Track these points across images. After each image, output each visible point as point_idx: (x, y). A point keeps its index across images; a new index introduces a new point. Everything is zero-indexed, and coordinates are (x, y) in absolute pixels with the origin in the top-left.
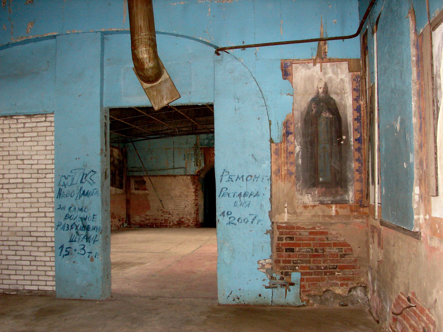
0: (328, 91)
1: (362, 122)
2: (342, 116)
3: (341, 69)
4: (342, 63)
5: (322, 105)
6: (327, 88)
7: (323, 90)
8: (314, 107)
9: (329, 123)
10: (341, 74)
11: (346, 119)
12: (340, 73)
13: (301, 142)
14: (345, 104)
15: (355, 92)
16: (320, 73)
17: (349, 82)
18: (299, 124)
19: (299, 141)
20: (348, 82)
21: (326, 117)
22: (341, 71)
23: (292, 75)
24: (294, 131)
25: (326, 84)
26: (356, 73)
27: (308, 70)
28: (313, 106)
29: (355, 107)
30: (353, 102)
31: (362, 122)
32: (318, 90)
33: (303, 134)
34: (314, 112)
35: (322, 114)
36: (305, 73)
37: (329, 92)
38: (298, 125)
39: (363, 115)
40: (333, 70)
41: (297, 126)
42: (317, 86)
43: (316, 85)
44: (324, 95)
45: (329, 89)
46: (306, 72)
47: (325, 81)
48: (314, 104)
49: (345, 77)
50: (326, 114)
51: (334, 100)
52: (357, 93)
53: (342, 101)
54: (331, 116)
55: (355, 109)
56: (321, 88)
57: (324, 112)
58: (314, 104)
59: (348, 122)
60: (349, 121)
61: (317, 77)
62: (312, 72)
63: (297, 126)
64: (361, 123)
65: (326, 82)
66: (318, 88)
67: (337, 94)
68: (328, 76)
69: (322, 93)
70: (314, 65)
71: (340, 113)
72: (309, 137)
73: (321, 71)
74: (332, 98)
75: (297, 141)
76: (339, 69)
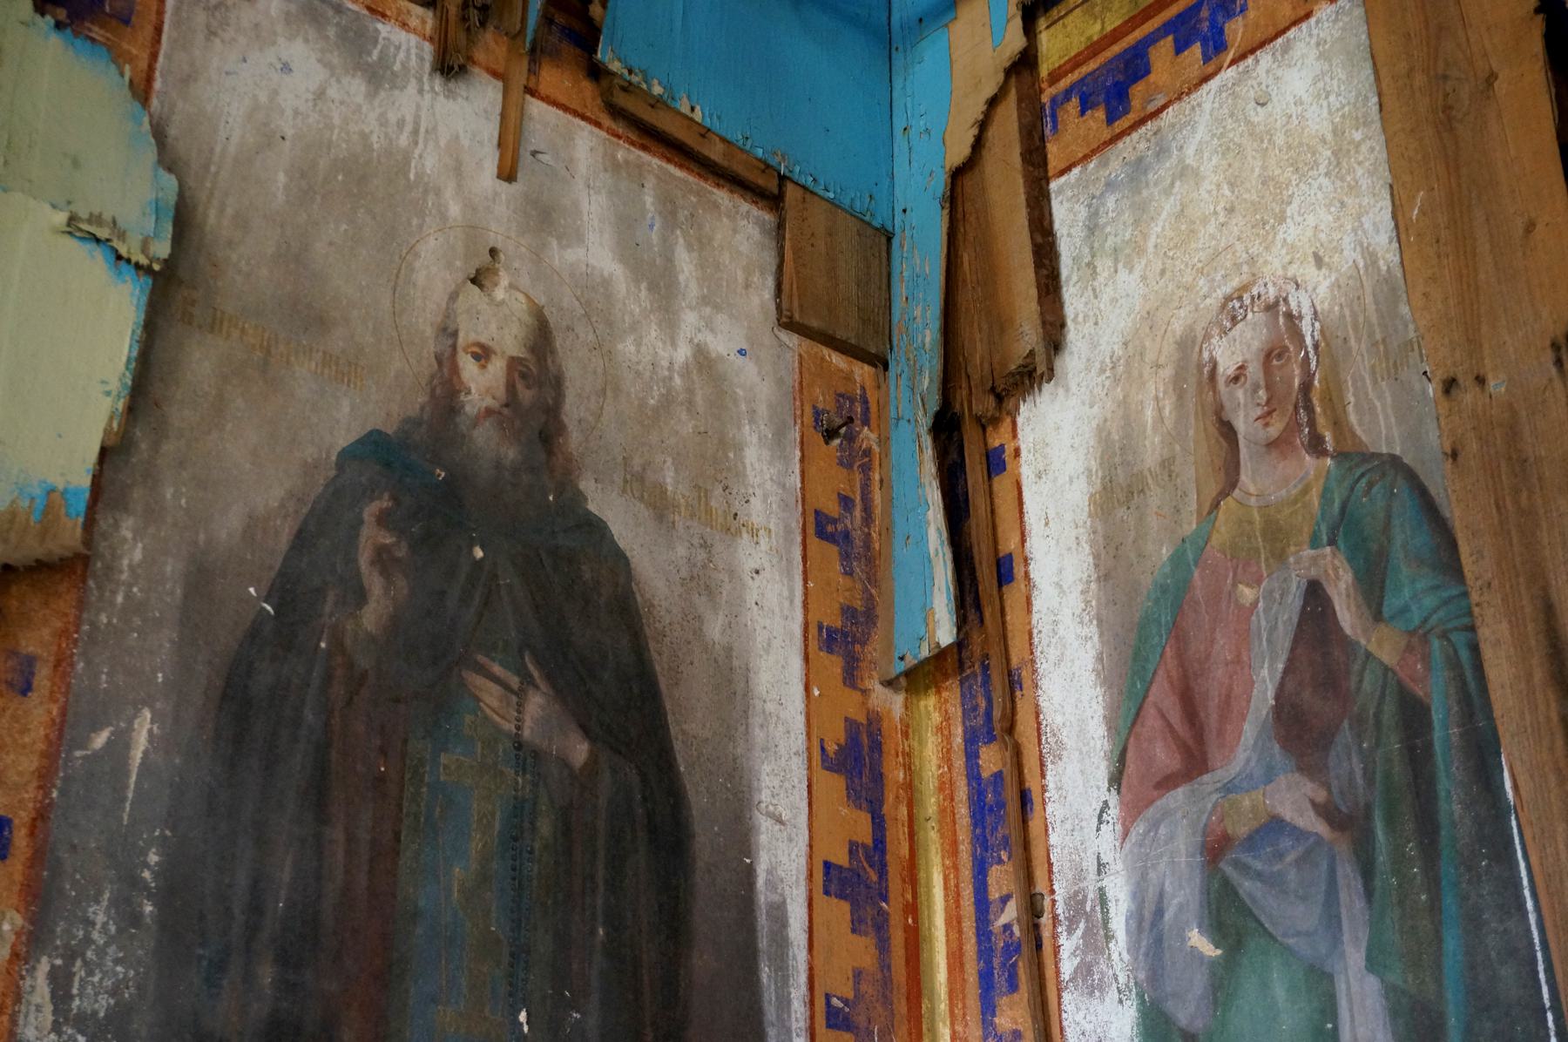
0: (561, 429)
1: (897, 938)
2: (698, 798)
3: (701, 244)
4: (722, 196)
5: (479, 564)
6: (558, 383)
7: (511, 387)
8: (382, 558)
9: (545, 827)
10: (705, 300)
11: (742, 840)
12: (693, 291)
13: (120, 1016)
14: (729, 650)
15: (833, 551)
16: (485, 177)
17: (780, 434)
18: (143, 730)
19: (103, 1004)
20: (763, 410)
21: (519, 745)
22: (701, 266)
23: (149, 30)
24: (41, 816)
25: (542, 336)
26: (837, 360)
27: (357, 86)
28: (371, 536)
29: (835, 736)
30: (806, 659)
31: (897, 938)
32: (447, 363)
33: (172, 891)
34: (372, 617)
35: (477, 680)
36: (320, 95)
37: (574, 439)
38: (120, 743)
39: (905, 851)
40: (626, 227)
41: (100, 740)
42: (449, 314)
43: (439, 296)
44: (511, 454)
45: (573, 410)
46: (332, 92)
47: (542, 300)
48: (383, 520)
49: (742, 352)
50: (521, 694)
51: (620, 558)
52: (849, 573)
53: (700, 602)
54: (580, 751)
55: (832, 748)
56: (483, 354)
57: (497, 669)
58: (383, 520)
59: (761, 882)
60: (772, 885)
61: (454, 210)
62: (401, 124)
63: (100, 740)
64: (883, 946)
65: (553, 318)
66: (448, 332)
67: (660, 507)
68: (565, 257)
69: (489, 412)
70: (450, 66)
71: (678, 746)
72: (266, 974)
73: (508, 174)
74: (595, 528)
75: (61, 995)
76: (690, 248)
